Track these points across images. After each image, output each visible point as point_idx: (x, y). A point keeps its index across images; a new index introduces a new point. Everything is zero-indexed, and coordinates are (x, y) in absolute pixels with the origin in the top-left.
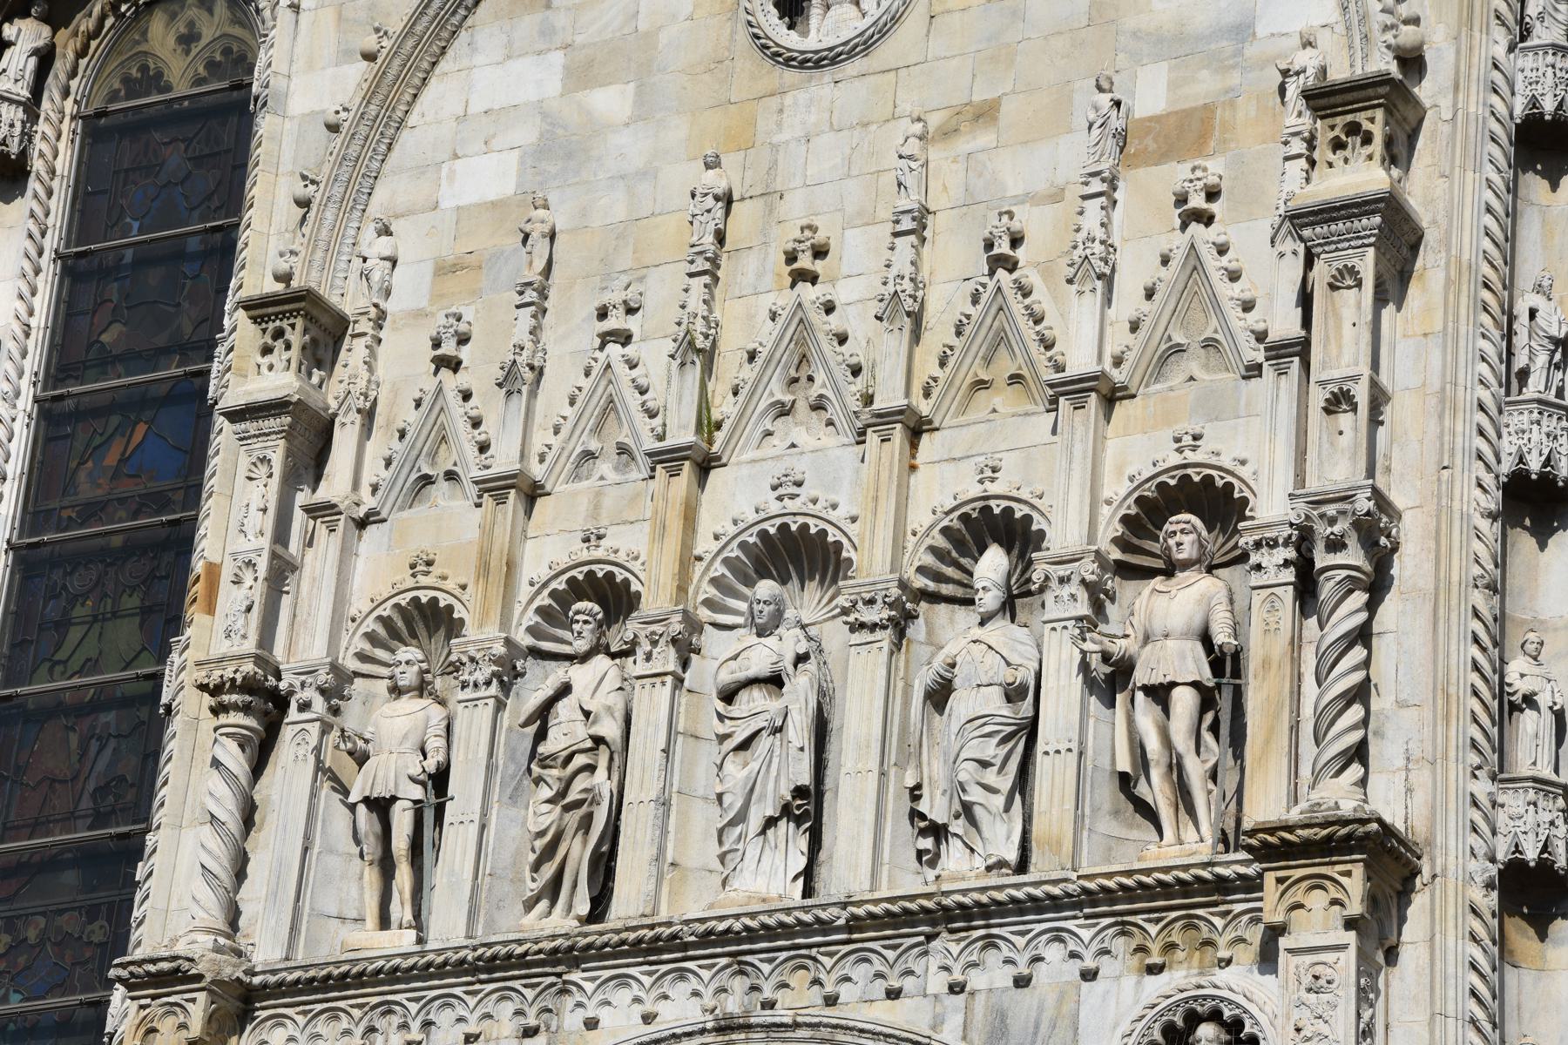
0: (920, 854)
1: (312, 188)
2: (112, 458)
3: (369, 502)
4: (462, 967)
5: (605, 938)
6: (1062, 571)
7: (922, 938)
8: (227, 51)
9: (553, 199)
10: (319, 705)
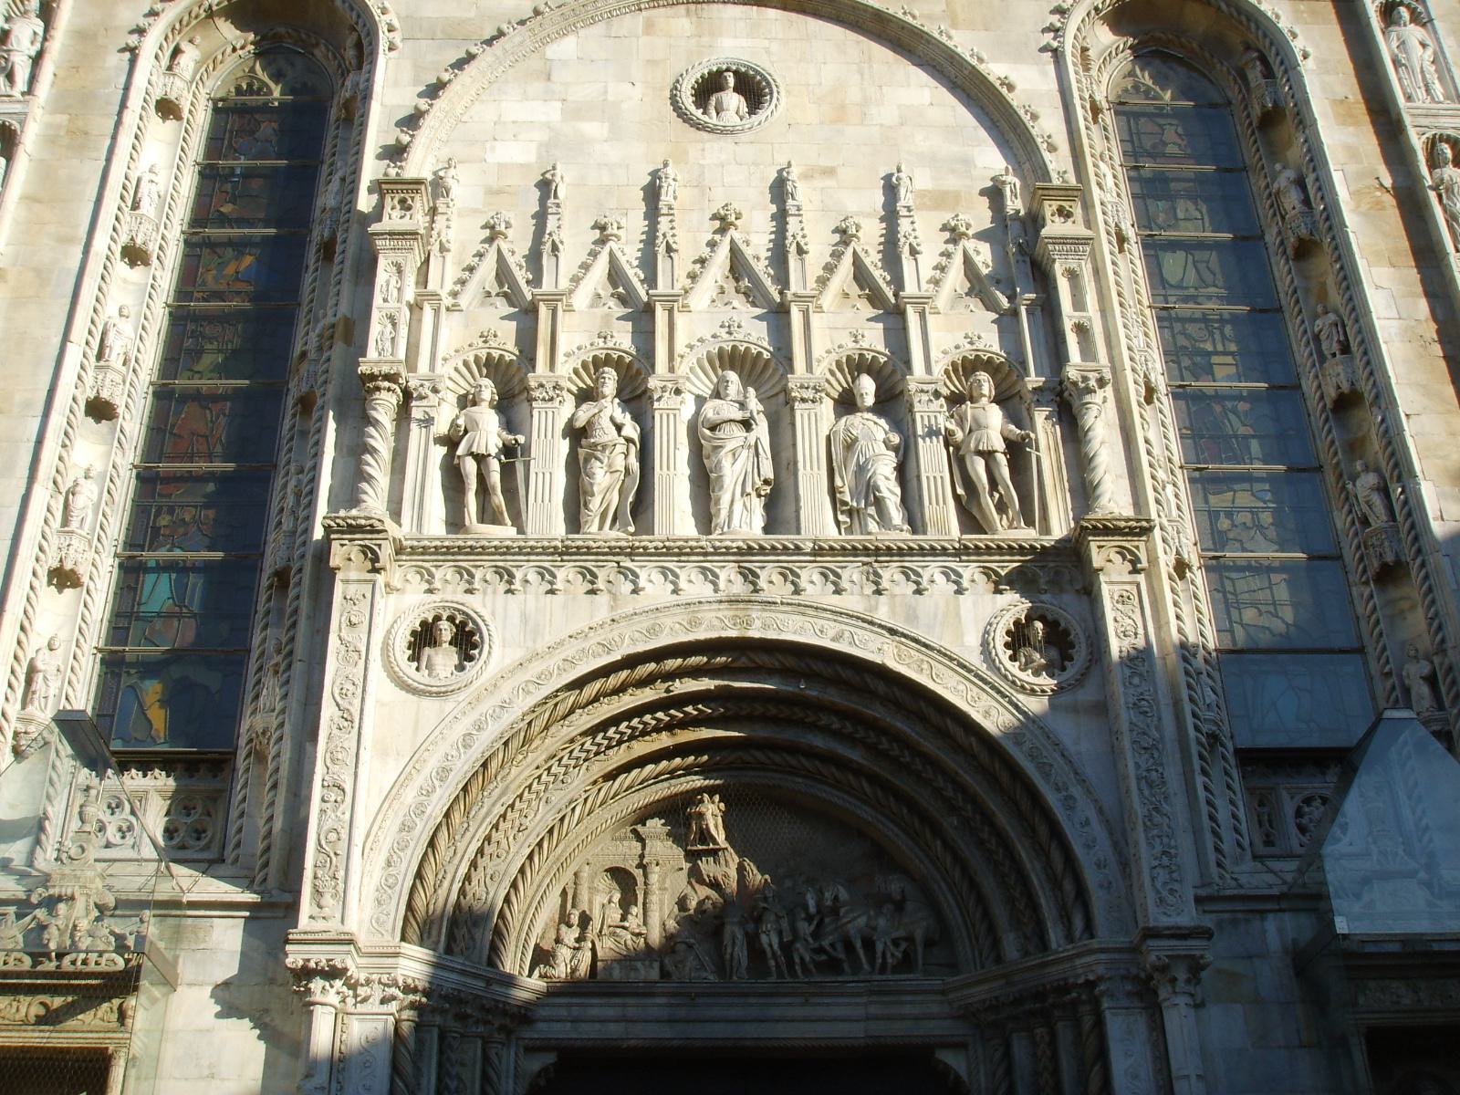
0: (838, 523)
2: (230, 270)
6: (925, 387)
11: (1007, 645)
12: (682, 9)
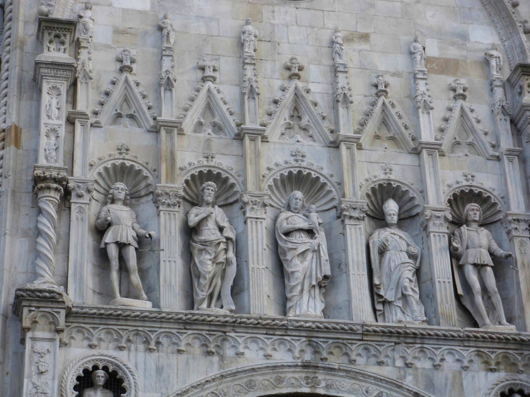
0: (375, 310)
3: (92, 120)
5: (251, 321)
6: (437, 214)
7: (393, 344)
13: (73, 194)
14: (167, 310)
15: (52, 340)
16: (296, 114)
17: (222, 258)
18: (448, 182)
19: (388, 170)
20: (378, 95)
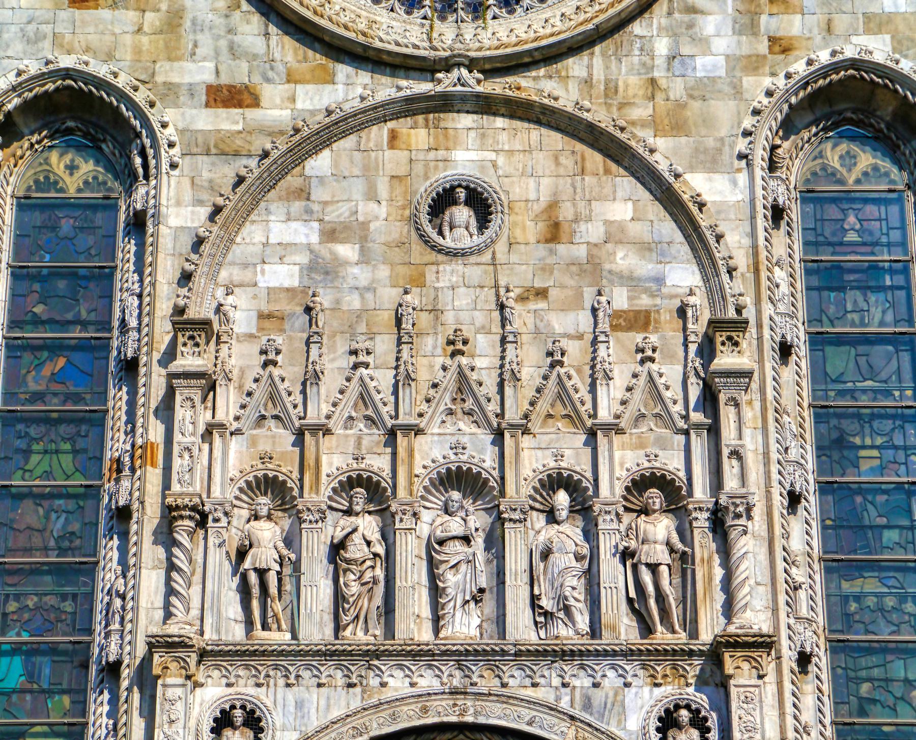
0: (536, 623)
1: (193, 267)
2: (47, 371)
3: (235, 425)
4: (318, 653)
5: (395, 647)
6: (607, 508)
8: (95, 178)
9: (320, 291)
10: (224, 522)
11: (658, 730)
12: (420, 118)
13: (210, 518)
14: (306, 642)
15: (184, 685)
16: (459, 396)
17: (368, 576)
18: (628, 465)
19: (558, 457)
20: (552, 366)
